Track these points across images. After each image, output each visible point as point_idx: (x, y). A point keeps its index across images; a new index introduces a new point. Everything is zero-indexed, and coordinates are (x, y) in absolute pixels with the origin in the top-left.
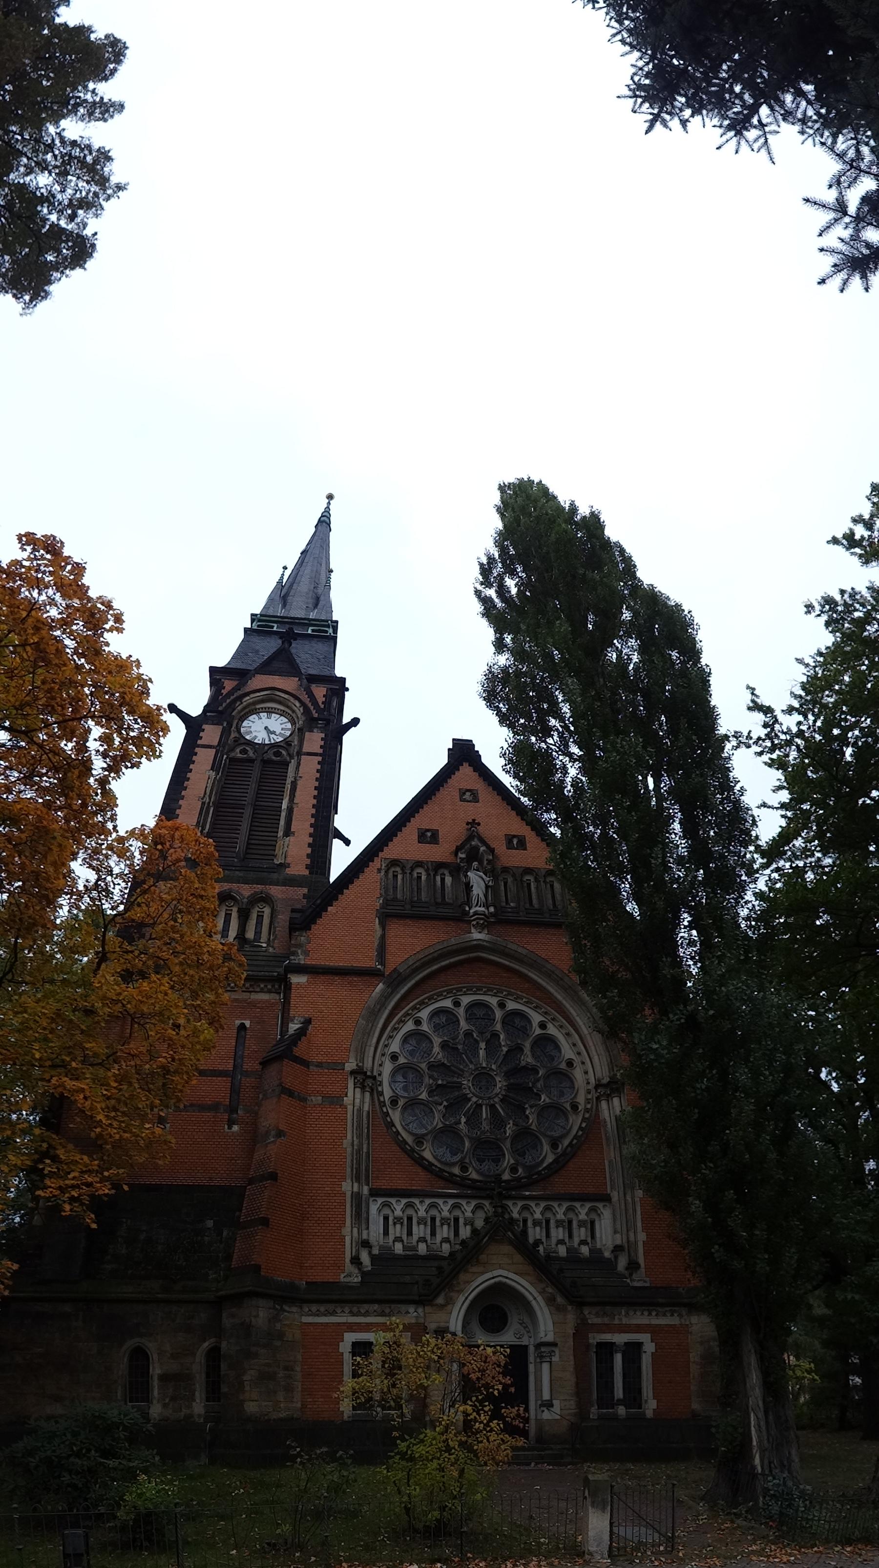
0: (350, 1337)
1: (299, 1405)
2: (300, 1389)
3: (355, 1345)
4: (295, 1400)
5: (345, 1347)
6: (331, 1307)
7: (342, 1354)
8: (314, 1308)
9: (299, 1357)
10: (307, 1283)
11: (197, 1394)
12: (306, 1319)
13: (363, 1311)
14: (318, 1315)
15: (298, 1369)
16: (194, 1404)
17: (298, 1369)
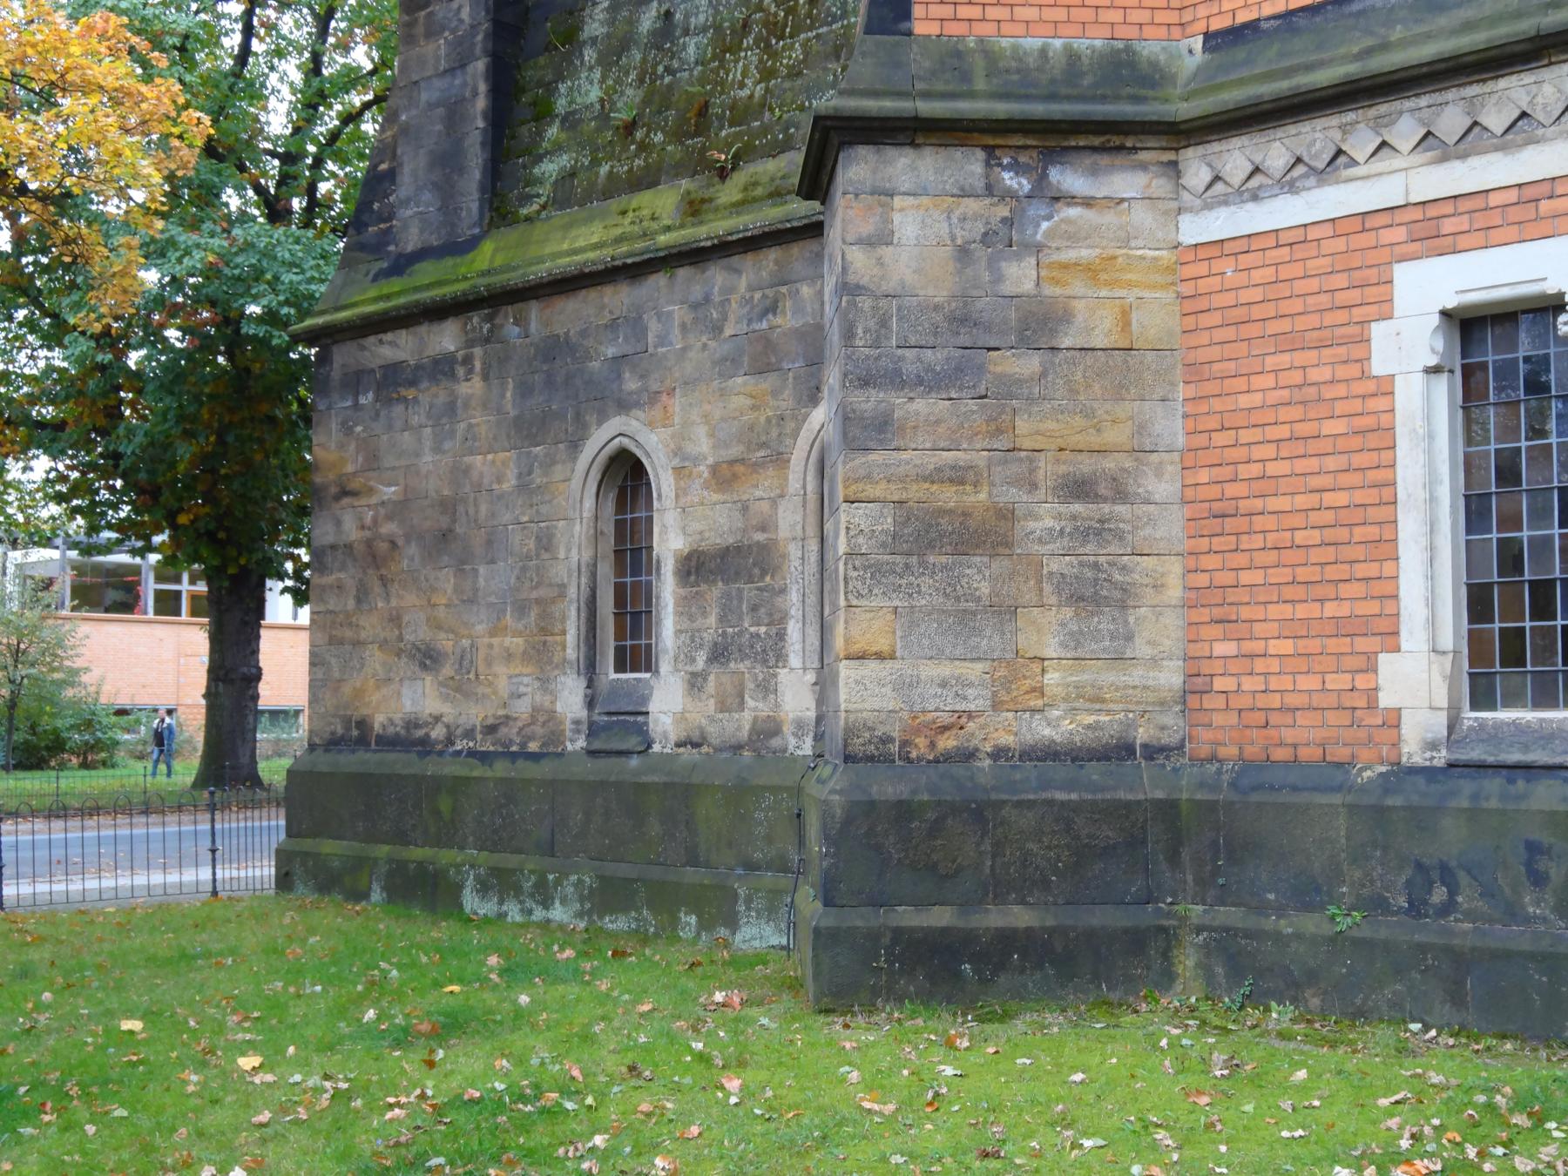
0: (1431, 287)
1: (1170, 677)
2: (1175, 593)
3: (1470, 325)
4: (1141, 648)
5: (1406, 344)
6: (1316, 135)
7: (1386, 387)
8: (1235, 156)
9: (1170, 428)
10: (1208, 36)
11: (793, 629)
12: (1199, 228)
13: (1496, 120)
14: (1255, 198)
15: (1163, 487)
16: (782, 672)
17: (1163, 487)
